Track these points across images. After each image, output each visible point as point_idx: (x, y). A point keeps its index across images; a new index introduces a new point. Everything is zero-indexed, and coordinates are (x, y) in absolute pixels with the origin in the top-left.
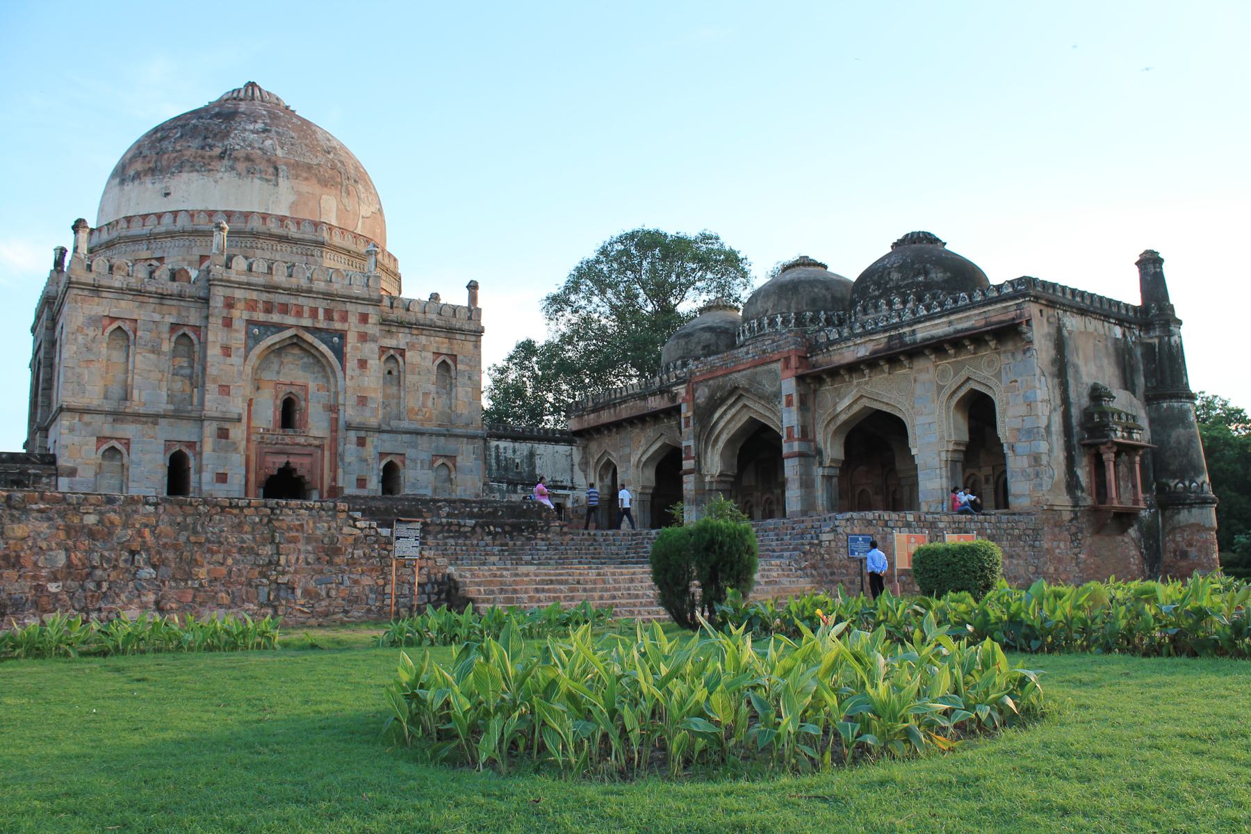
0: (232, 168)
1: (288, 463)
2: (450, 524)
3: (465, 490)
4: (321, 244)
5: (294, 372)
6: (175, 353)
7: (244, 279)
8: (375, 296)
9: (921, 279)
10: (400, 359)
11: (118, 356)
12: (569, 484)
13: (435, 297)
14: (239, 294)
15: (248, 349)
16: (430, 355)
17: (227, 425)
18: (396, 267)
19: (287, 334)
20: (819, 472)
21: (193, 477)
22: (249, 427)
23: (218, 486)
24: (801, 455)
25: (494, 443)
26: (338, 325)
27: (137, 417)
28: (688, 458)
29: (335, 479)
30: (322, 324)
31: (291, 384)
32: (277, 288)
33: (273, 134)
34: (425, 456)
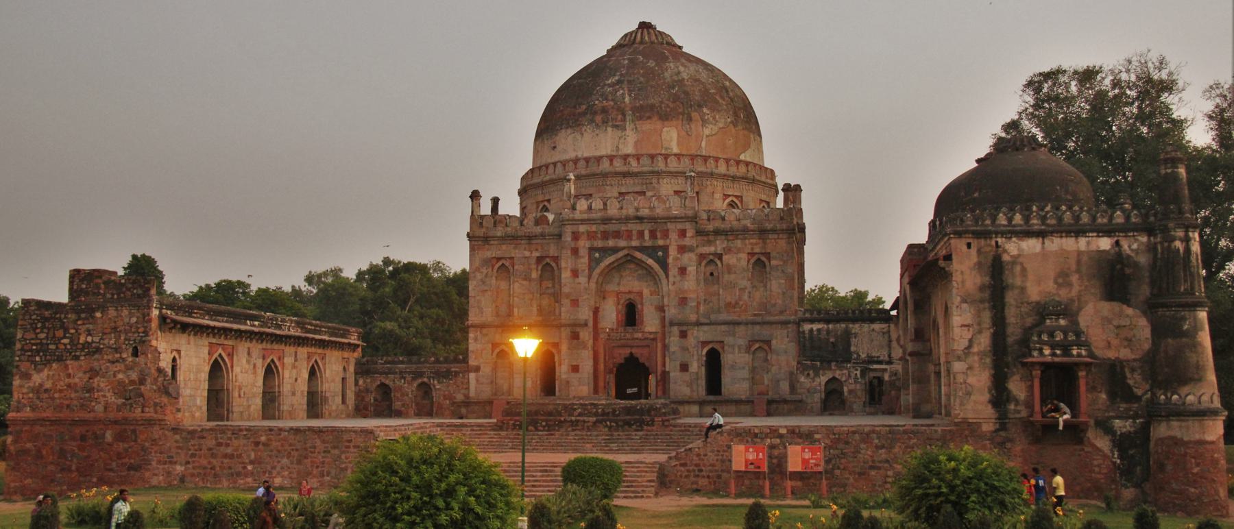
0: (592, 121)
2: (577, 421)
4: (658, 174)
5: (631, 283)
7: (585, 216)
8: (690, 213)
9: (976, 195)
10: (718, 262)
11: (503, 285)
12: (887, 358)
14: (582, 228)
15: (591, 269)
16: (744, 256)
17: (578, 329)
19: (621, 254)
20: (931, 368)
23: (573, 375)
24: (910, 354)
25: (807, 327)
26: (661, 242)
29: (664, 365)
30: (648, 242)
31: (630, 292)
33: (625, 85)
34: (742, 342)
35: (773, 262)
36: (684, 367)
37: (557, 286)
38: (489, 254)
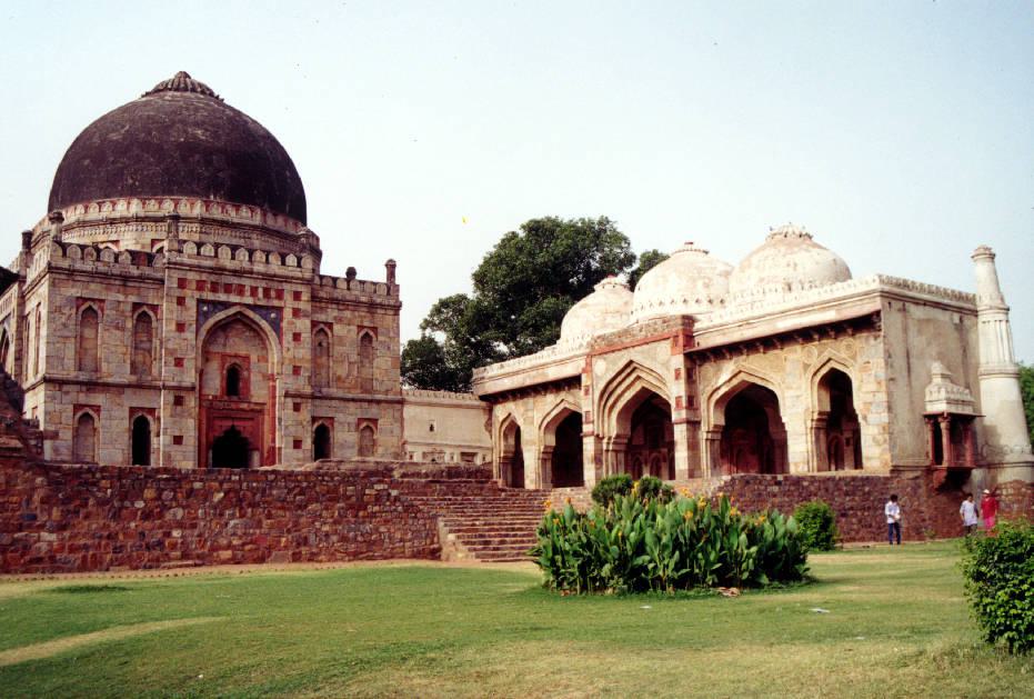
1: (233, 426)
3: (386, 450)
5: (238, 345)
6: (135, 327)
7: (195, 262)
8: (308, 275)
11: (88, 333)
13: (351, 272)
14: (192, 276)
16: (354, 328)
18: (318, 245)
19: (232, 311)
21: (154, 440)
22: (200, 395)
26: (276, 303)
27: (106, 387)
28: (588, 423)
31: (236, 356)
32: (225, 270)
34: (353, 419)
35: (381, 338)
36: (297, 444)
37: (156, 342)
38: (74, 291)
